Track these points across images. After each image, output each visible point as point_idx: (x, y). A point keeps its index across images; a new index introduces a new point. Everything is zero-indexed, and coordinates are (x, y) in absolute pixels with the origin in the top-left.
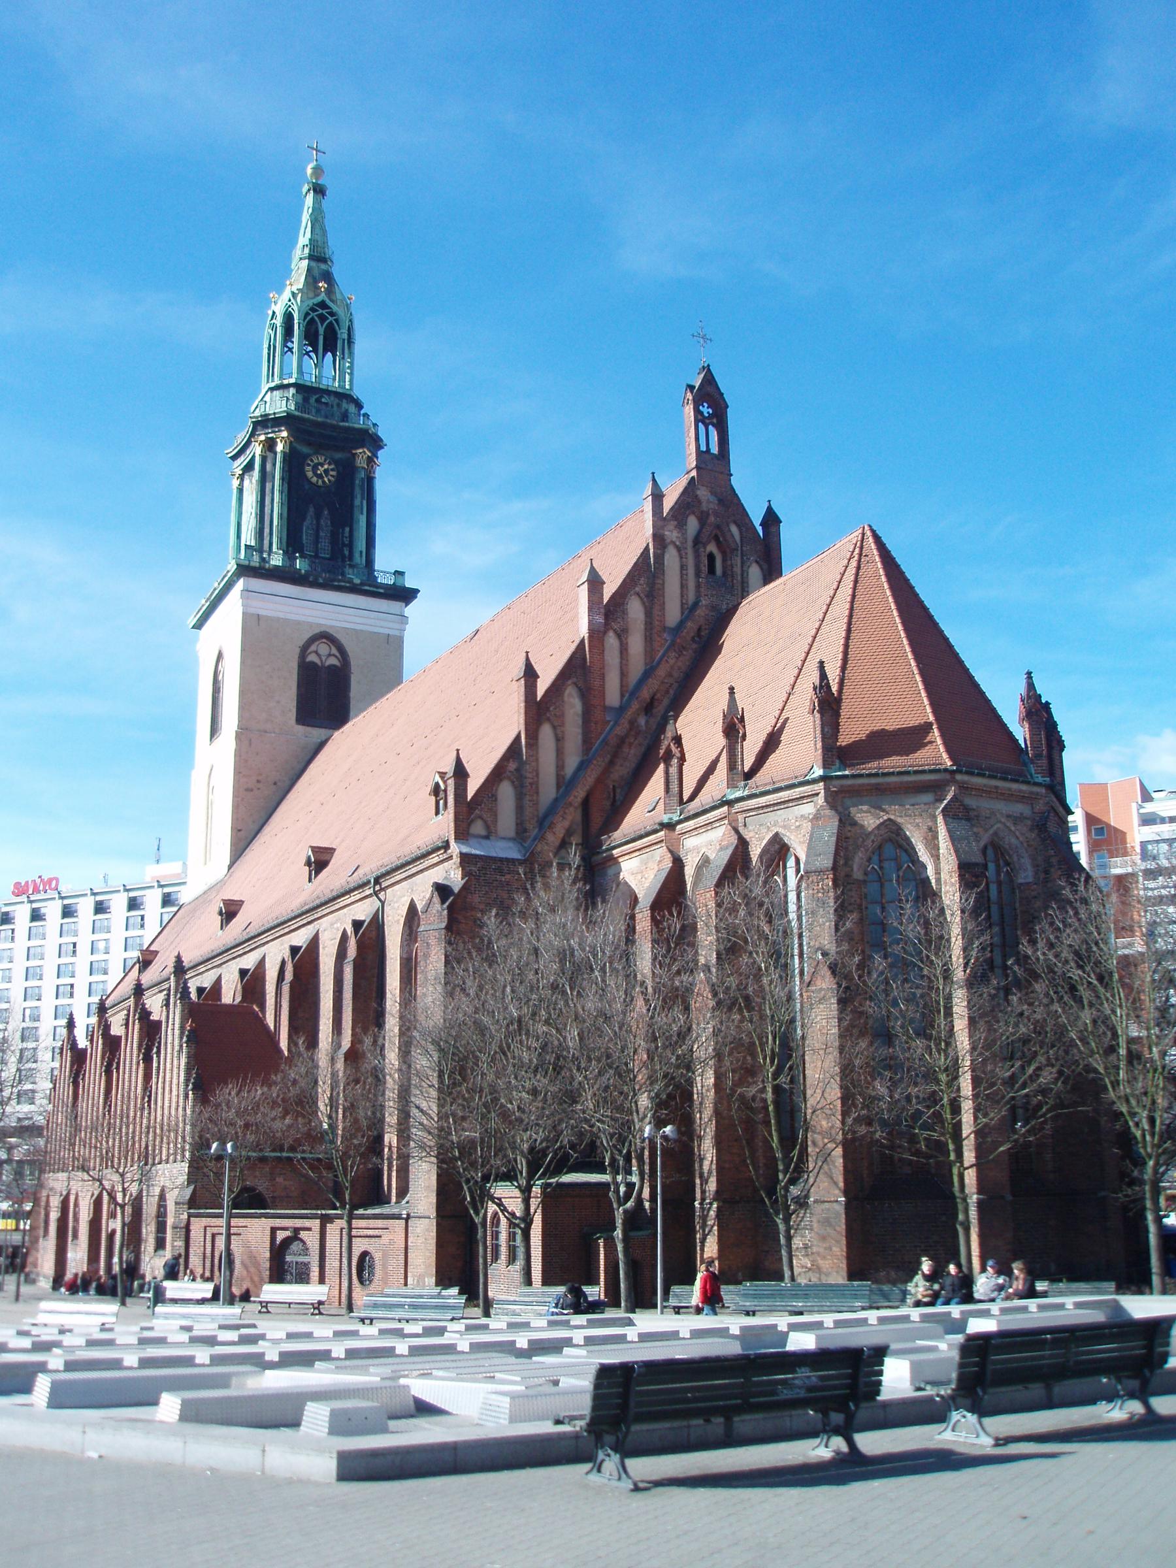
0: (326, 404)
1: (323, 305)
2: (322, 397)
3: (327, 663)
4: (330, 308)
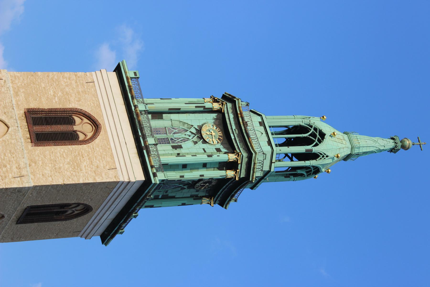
1: (323, 135)
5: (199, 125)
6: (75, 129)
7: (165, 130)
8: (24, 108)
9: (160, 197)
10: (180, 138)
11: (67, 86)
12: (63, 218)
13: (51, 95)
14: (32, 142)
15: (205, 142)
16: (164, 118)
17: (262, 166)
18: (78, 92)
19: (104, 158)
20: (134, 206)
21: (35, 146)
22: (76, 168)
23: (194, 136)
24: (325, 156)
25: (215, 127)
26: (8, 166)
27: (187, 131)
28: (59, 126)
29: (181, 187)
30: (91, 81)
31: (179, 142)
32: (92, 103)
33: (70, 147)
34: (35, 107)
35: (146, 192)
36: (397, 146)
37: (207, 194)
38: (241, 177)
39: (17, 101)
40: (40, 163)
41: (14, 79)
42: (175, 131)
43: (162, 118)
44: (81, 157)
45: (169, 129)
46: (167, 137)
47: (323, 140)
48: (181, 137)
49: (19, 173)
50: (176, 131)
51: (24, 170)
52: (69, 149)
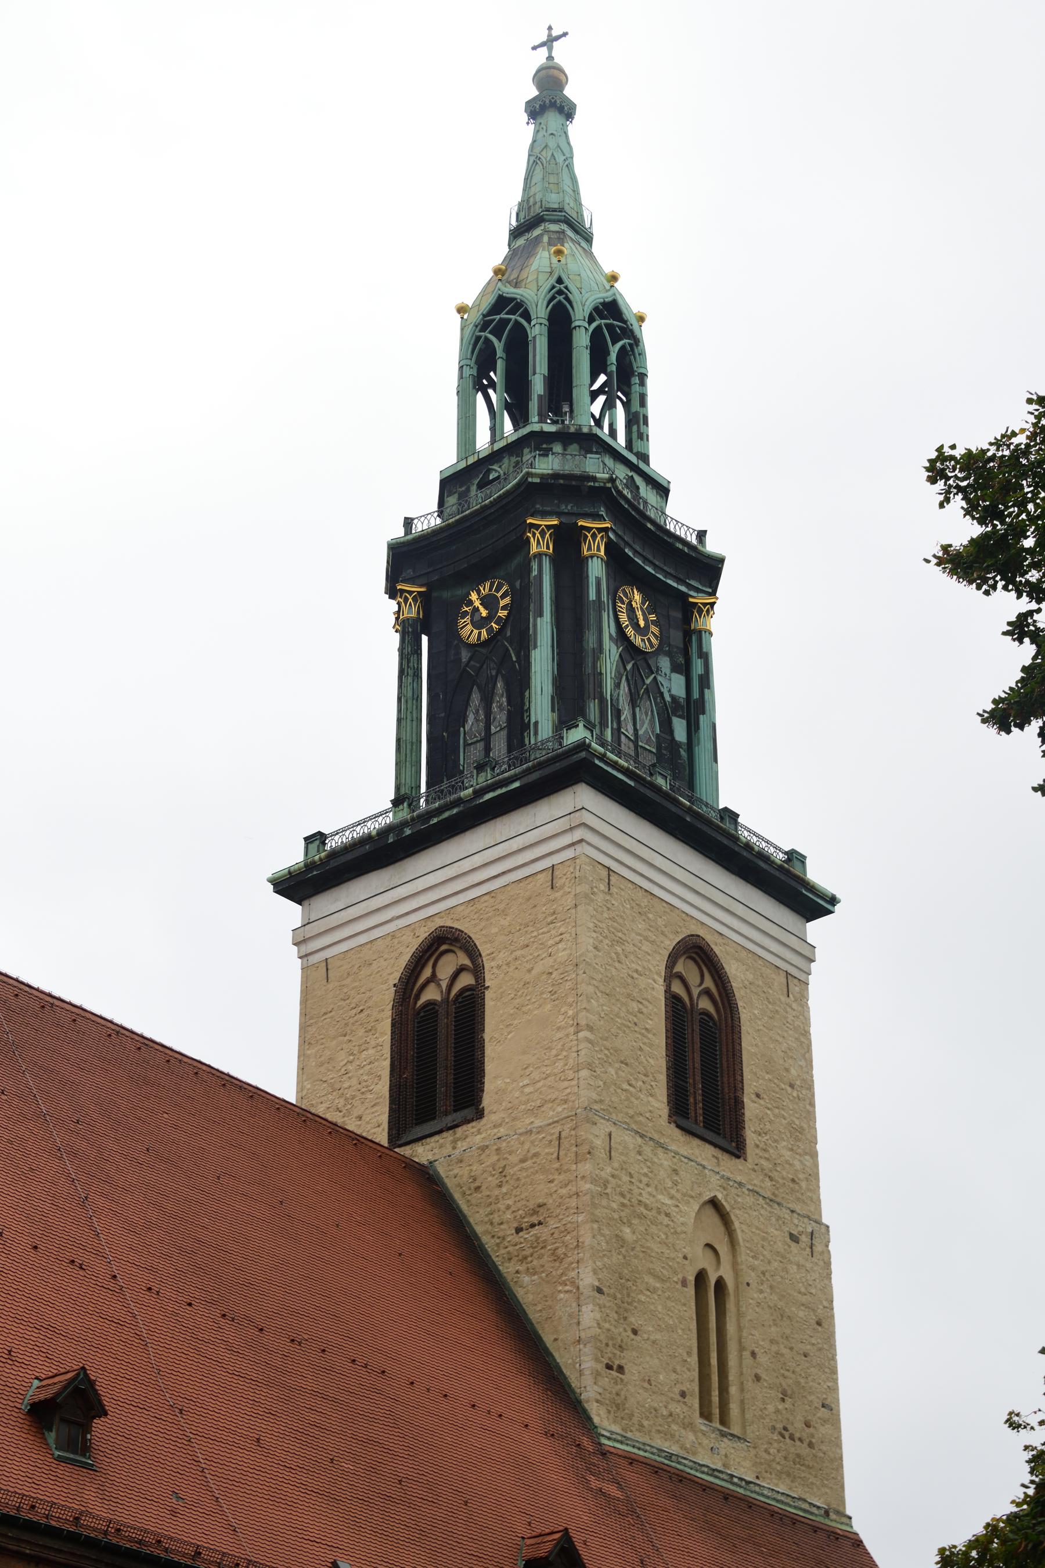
0: (498, 478)
1: (502, 303)
2: (489, 471)
3: (455, 991)
4: (513, 299)
36: (550, 101)
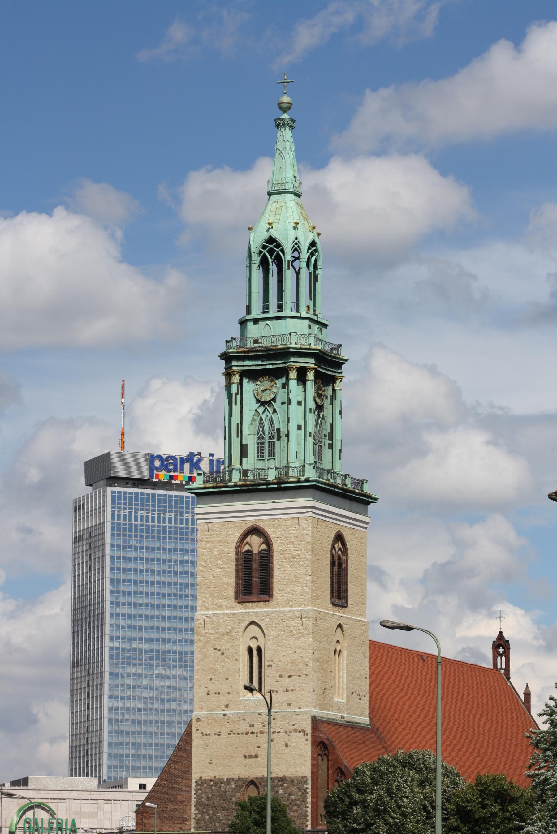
1: (271, 240)
5: (255, 402)
6: (257, 552)
7: (260, 445)
8: (234, 602)
9: (330, 442)
10: (269, 428)
11: (212, 552)
12: (345, 558)
13: (221, 572)
14: (268, 601)
15: (274, 399)
16: (247, 443)
17: (303, 336)
18: (219, 542)
19: (287, 528)
20: (338, 490)
21: (273, 598)
22: (296, 560)
23: (268, 410)
24: (296, 241)
25: (259, 383)
26: (292, 628)
27: (261, 419)
28: (253, 568)
29: (321, 421)
30: (207, 526)
31: (273, 430)
32: (231, 530)
33: (274, 562)
34: (234, 590)
35: (324, 486)
37: (331, 385)
38: (314, 362)
39: (228, 608)
40: (290, 595)
41: (205, 608)
42: (261, 432)
43: (247, 445)
44: (286, 552)
45: (259, 438)
46: (267, 443)
47: (277, 241)
48: (268, 426)
49: (299, 619)
50: (261, 430)
51: (295, 614)
52: (276, 564)
